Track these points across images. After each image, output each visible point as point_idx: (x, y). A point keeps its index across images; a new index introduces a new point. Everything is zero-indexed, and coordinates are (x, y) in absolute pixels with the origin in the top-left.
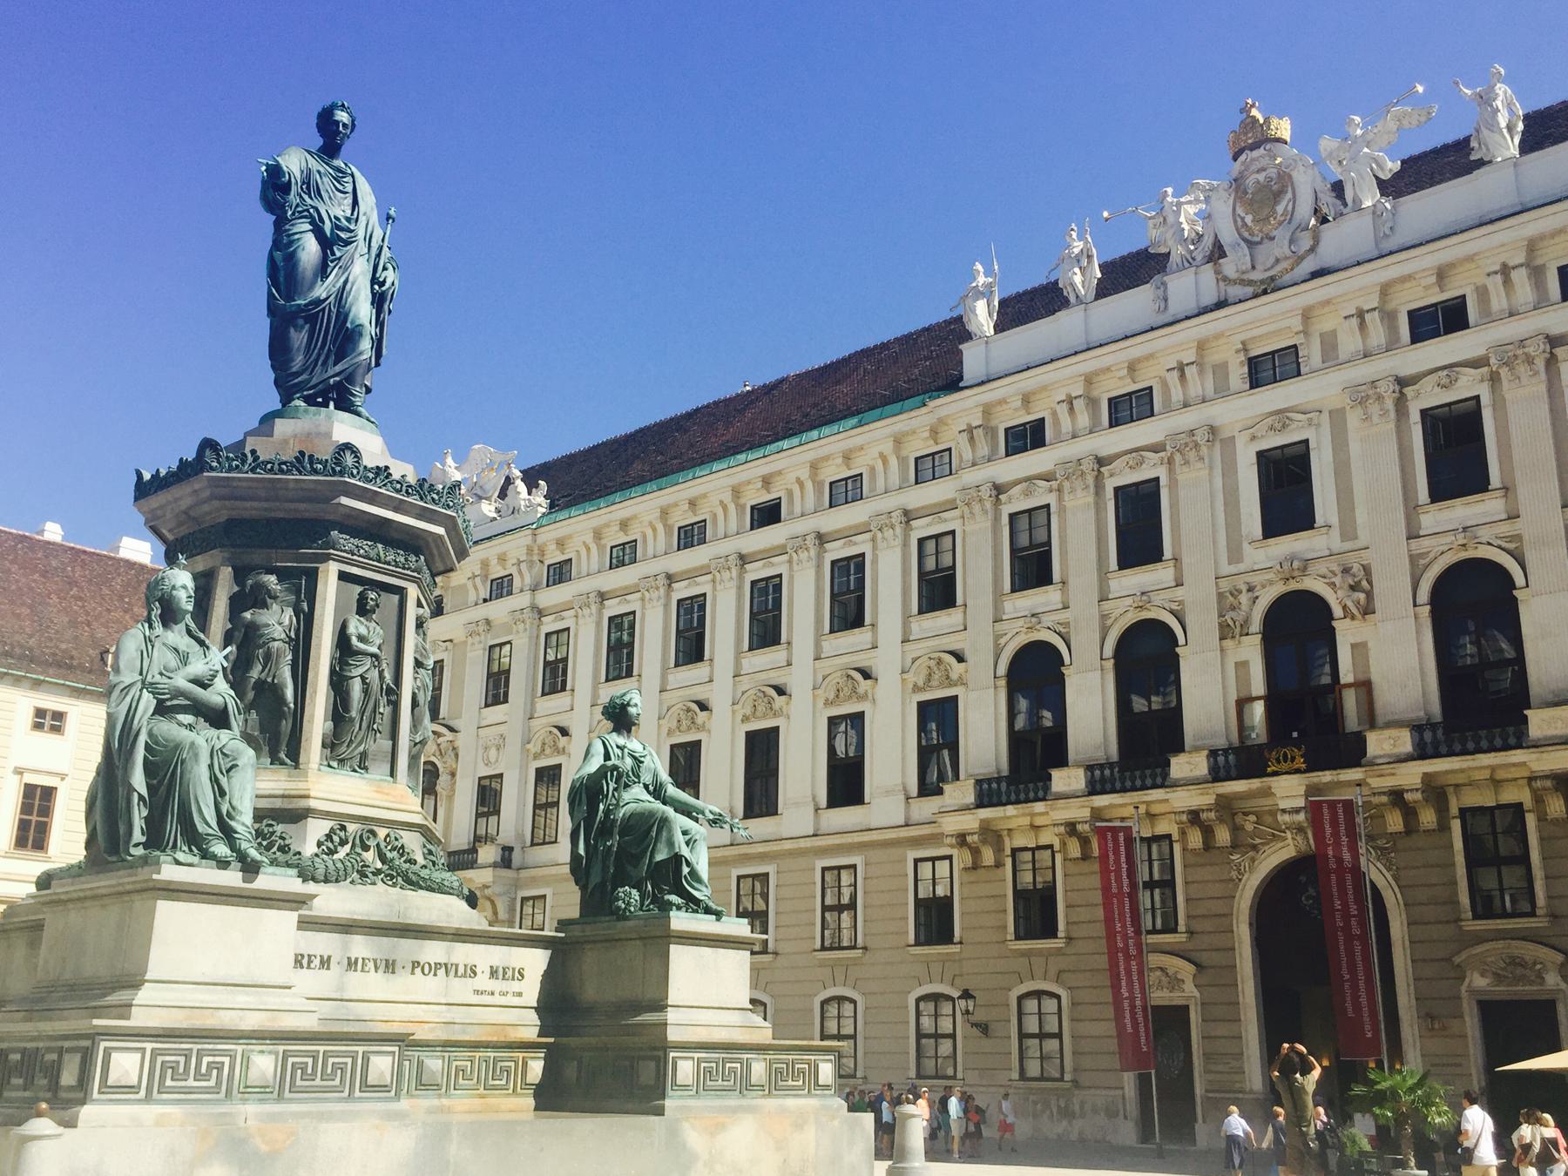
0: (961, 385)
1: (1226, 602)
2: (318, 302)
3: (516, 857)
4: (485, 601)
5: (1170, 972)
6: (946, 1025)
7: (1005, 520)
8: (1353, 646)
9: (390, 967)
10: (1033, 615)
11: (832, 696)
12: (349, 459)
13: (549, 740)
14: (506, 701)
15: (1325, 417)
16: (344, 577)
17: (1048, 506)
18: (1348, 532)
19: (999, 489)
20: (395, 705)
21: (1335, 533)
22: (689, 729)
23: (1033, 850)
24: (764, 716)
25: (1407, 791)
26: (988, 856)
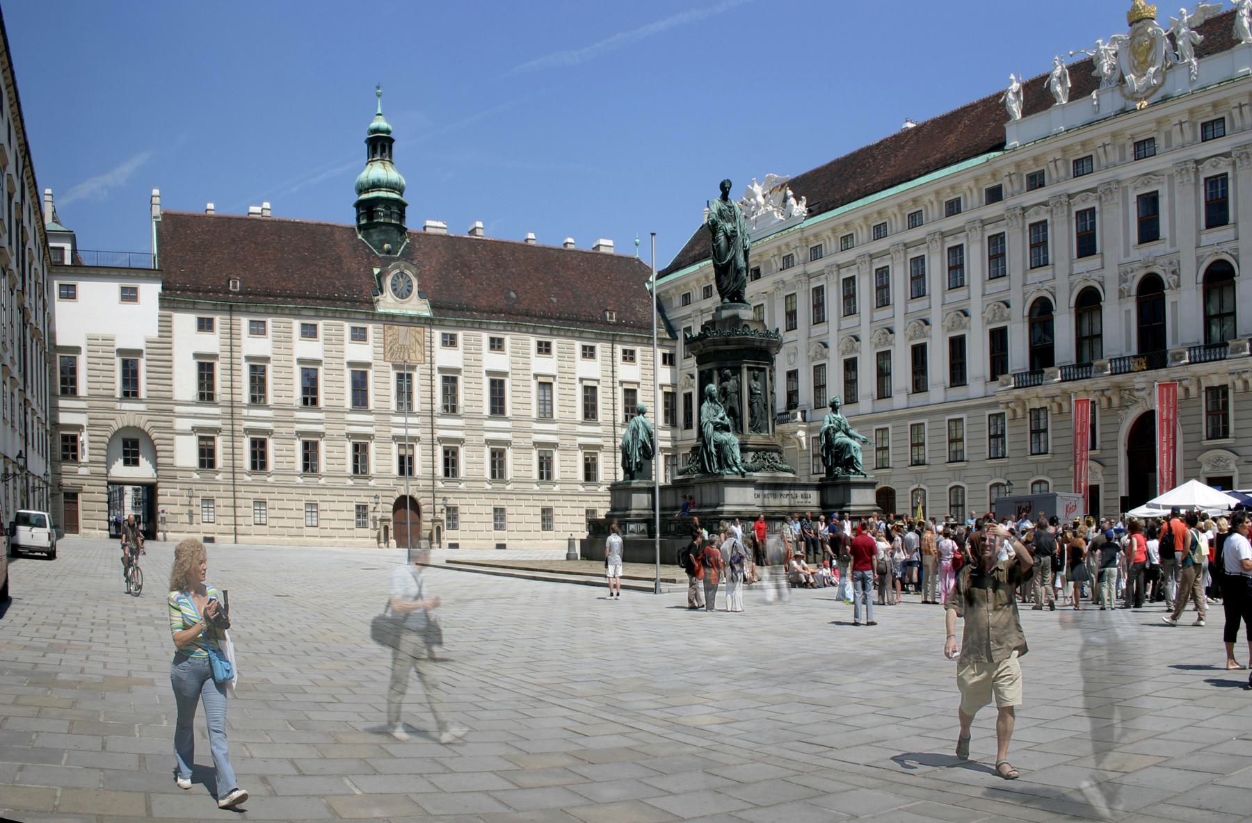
11: (950, 325)
14: (796, 328)
15: (1166, 178)
21: (1168, 242)
24: (919, 337)
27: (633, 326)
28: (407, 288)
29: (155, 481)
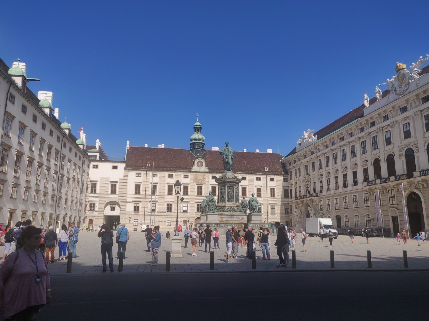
0: (364, 116)
1: (400, 151)
2: (226, 161)
3: (318, 194)
4: (311, 155)
5: (395, 211)
6: (348, 220)
7: (371, 138)
8: (417, 157)
9: (232, 218)
10: (376, 154)
12: (226, 178)
13: (320, 176)
15: (412, 117)
16: (227, 186)
17: (390, 130)
18: (416, 138)
19: (370, 133)
20: (233, 196)
21: (414, 138)
22: (328, 176)
23: (391, 190)
24: (345, 172)
25: (419, 182)
26: (372, 194)
27: (274, 172)
28: (201, 164)
29: (119, 215)
